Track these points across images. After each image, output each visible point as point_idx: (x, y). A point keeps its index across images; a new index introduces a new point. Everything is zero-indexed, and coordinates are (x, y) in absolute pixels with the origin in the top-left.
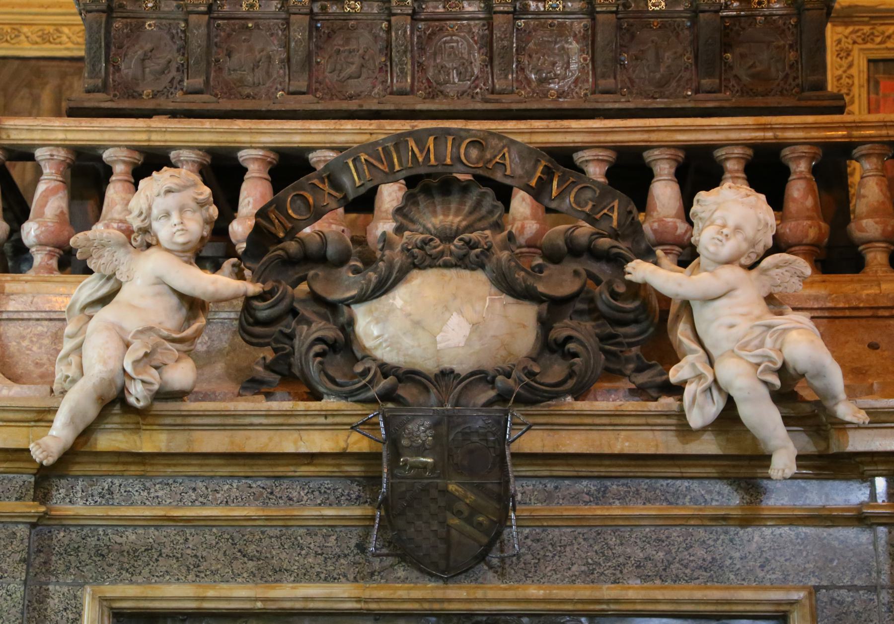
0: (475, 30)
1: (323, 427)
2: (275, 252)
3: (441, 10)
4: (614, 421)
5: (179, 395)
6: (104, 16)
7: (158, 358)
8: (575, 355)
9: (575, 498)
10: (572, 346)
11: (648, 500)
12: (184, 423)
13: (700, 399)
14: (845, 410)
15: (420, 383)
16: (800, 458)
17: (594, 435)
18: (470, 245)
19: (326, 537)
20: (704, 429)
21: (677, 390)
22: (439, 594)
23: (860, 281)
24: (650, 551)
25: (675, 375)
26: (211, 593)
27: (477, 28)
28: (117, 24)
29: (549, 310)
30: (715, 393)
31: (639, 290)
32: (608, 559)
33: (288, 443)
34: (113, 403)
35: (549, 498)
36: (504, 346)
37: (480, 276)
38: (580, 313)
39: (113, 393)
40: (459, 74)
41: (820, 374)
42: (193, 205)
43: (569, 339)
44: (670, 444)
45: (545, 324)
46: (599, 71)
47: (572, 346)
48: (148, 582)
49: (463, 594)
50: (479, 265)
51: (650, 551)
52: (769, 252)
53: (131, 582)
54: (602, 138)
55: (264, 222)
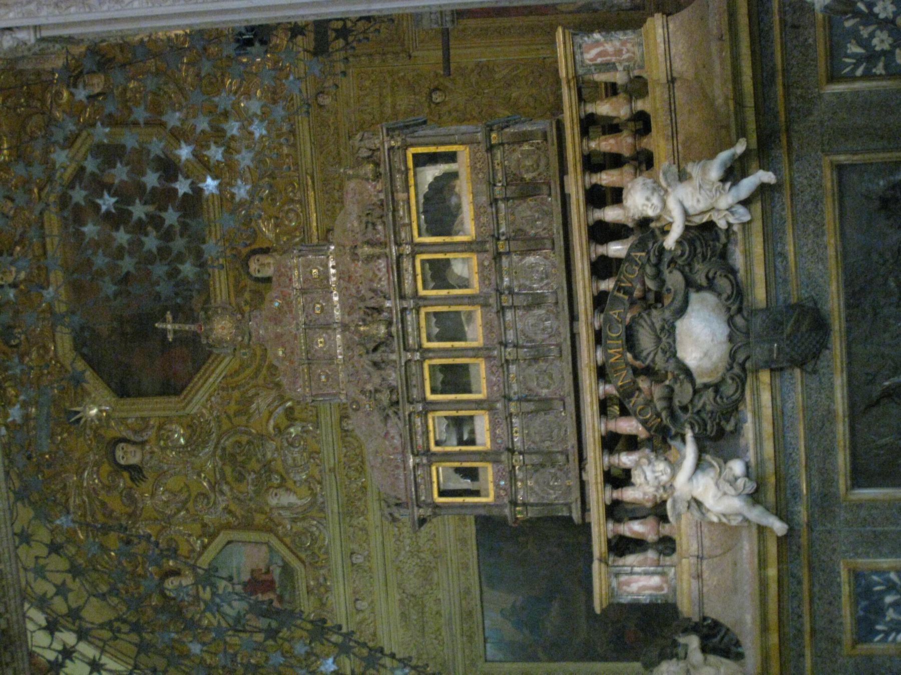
0: (520, 313)
1: (759, 395)
2: (667, 422)
3: (511, 331)
4: (747, 254)
5: (747, 466)
6: (529, 508)
7: (731, 478)
8: (715, 273)
9: (786, 269)
10: (711, 275)
11: (784, 232)
12: (760, 463)
13: (737, 216)
14: (740, 148)
15: (735, 352)
16: (762, 167)
17: (755, 262)
18: (663, 329)
19: (811, 389)
20: (750, 212)
21: (730, 225)
22: (837, 334)
23: (655, 117)
24: (810, 231)
25: (722, 224)
26: (842, 443)
27: (520, 313)
28: (532, 501)
29: (692, 287)
30: (733, 209)
31: (679, 242)
32: (815, 251)
33: (767, 412)
34: (754, 498)
35: (785, 281)
36: (714, 310)
37: (678, 324)
38: (691, 270)
39: (750, 500)
40: (546, 320)
41: (724, 164)
42: (650, 467)
43: (707, 277)
44: (757, 226)
45: (699, 289)
46: (539, 247)
47: (711, 275)
48: (837, 473)
49: (837, 322)
50: (673, 327)
51: (810, 231)
52: (656, 182)
53: (838, 482)
54: (585, 250)
55: (654, 429)
